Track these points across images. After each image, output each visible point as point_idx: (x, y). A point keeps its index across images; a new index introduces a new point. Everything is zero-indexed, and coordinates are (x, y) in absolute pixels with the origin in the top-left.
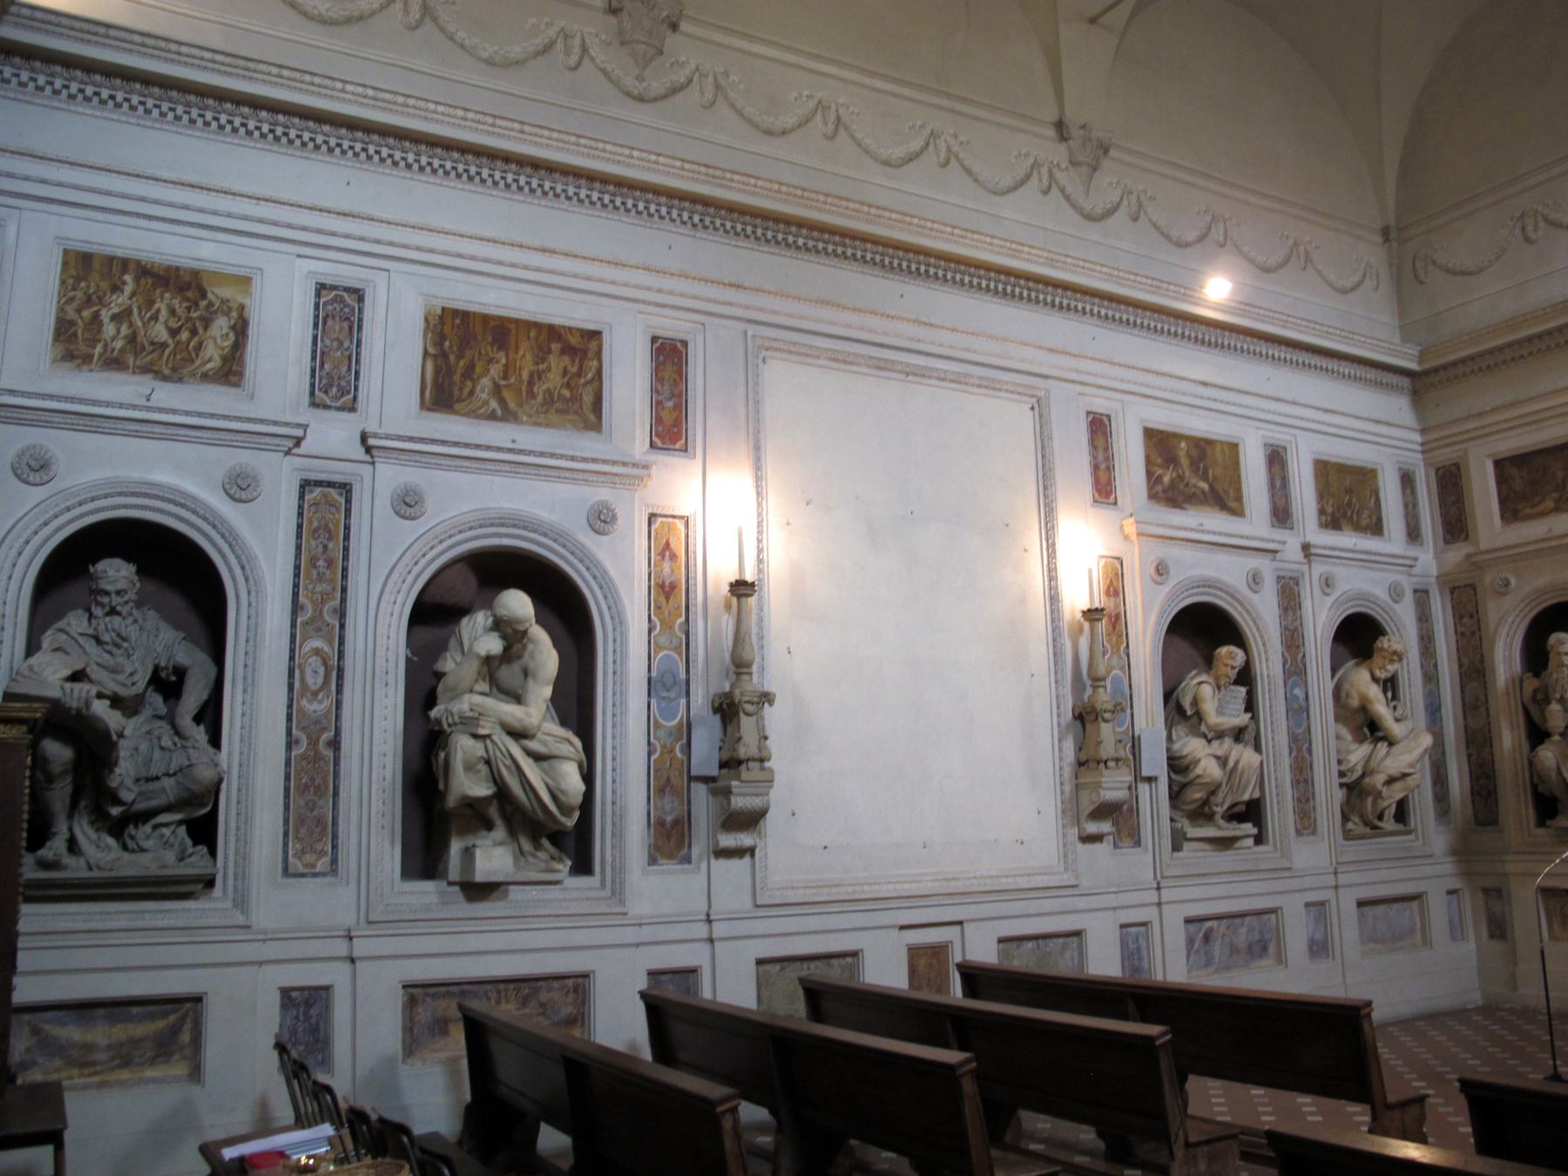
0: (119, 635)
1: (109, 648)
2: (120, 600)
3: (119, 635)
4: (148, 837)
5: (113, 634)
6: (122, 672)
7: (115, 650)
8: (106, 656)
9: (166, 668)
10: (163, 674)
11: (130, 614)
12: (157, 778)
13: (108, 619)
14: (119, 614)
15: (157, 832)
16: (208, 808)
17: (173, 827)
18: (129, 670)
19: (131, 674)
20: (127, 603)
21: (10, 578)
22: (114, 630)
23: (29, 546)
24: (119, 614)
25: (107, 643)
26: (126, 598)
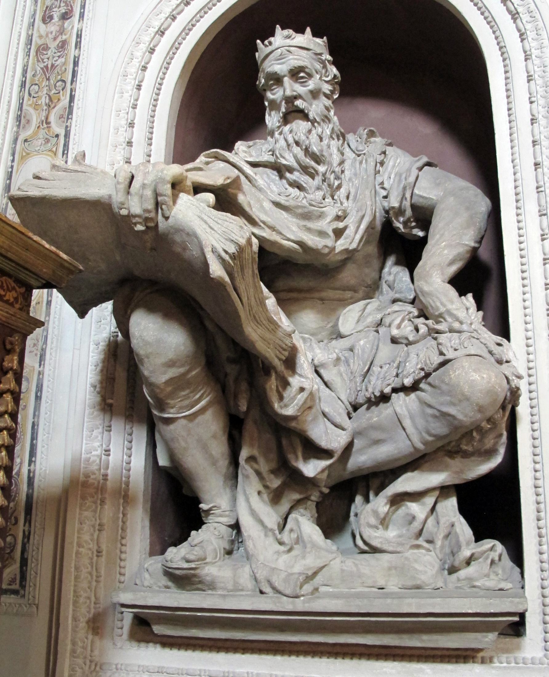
0: (307, 151)
1: (295, 176)
2: (299, 89)
3: (307, 151)
4: (384, 522)
5: (297, 150)
6: (321, 216)
7: (303, 179)
8: (295, 192)
9: (400, 212)
10: (399, 225)
11: (326, 119)
12: (384, 398)
13: (287, 128)
14: (303, 115)
15: (402, 511)
16: (497, 460)
17: (429, 500)
18: (331, 211)
19: (338, 218)
20: (315, 94)
21: (139, 87)
22: (297, 143)
23: (164, 39)
24: (303, 115)
25: (290, 170)
26: (311, 85)
